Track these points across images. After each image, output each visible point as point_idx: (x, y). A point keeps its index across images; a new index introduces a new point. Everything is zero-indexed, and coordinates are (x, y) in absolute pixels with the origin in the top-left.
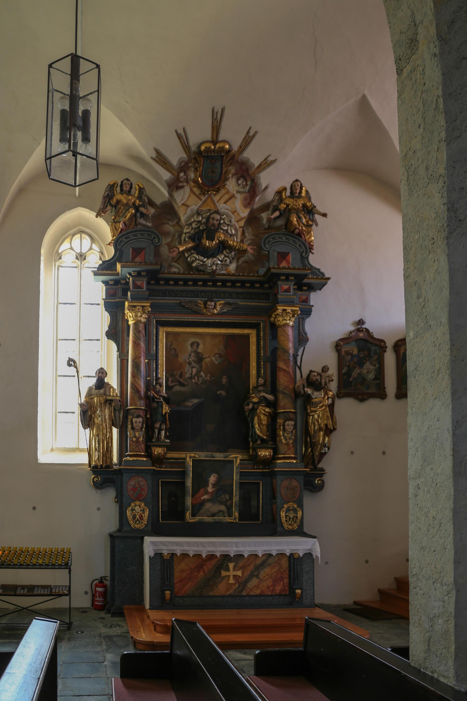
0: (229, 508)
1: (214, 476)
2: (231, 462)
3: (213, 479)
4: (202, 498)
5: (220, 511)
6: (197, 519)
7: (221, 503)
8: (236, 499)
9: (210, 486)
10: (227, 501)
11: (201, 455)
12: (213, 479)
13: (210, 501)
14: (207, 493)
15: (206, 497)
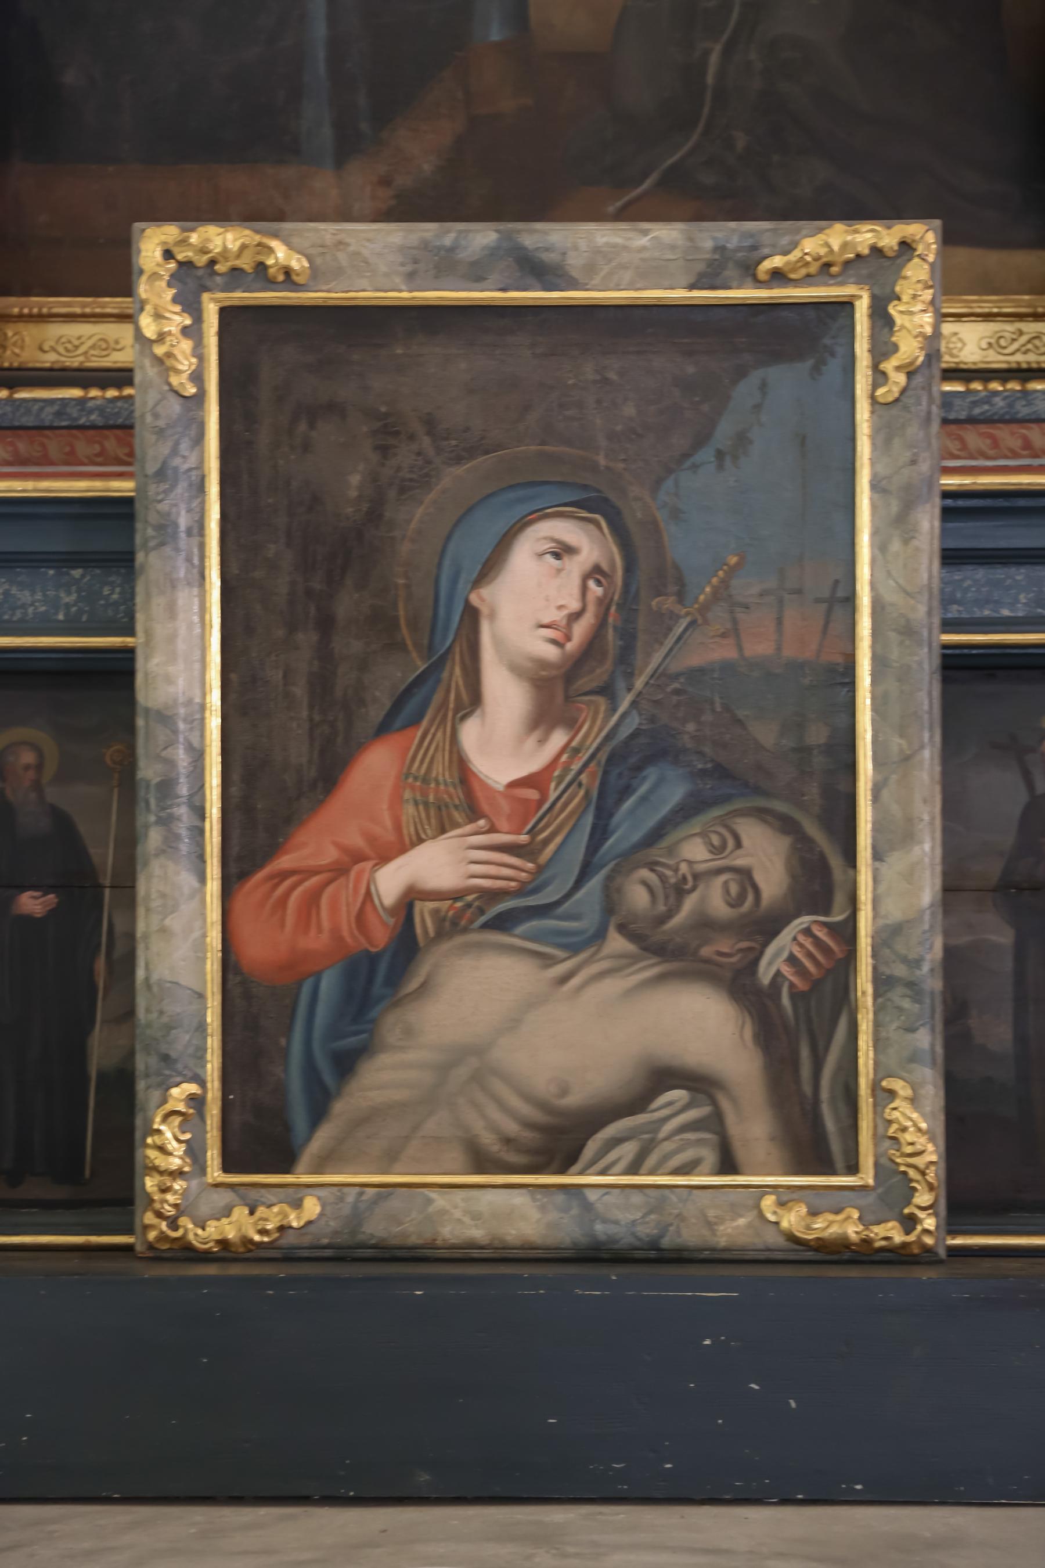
0: (799, 1029)
1: (562, 551)
2: (808, 334)
3: (536, 592)
4: (390, 881)
5: (662, 1077)
6: (300, 1205)
7: (671, 953)
8: (897, 882)
9: (505, 696)
10: (766, 926)
11: (358, 258)
12: (536, 592)
13: (502, 923)
14: (461, 800)
15: (439, 864)
